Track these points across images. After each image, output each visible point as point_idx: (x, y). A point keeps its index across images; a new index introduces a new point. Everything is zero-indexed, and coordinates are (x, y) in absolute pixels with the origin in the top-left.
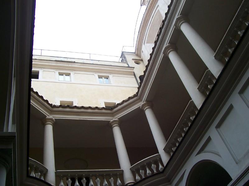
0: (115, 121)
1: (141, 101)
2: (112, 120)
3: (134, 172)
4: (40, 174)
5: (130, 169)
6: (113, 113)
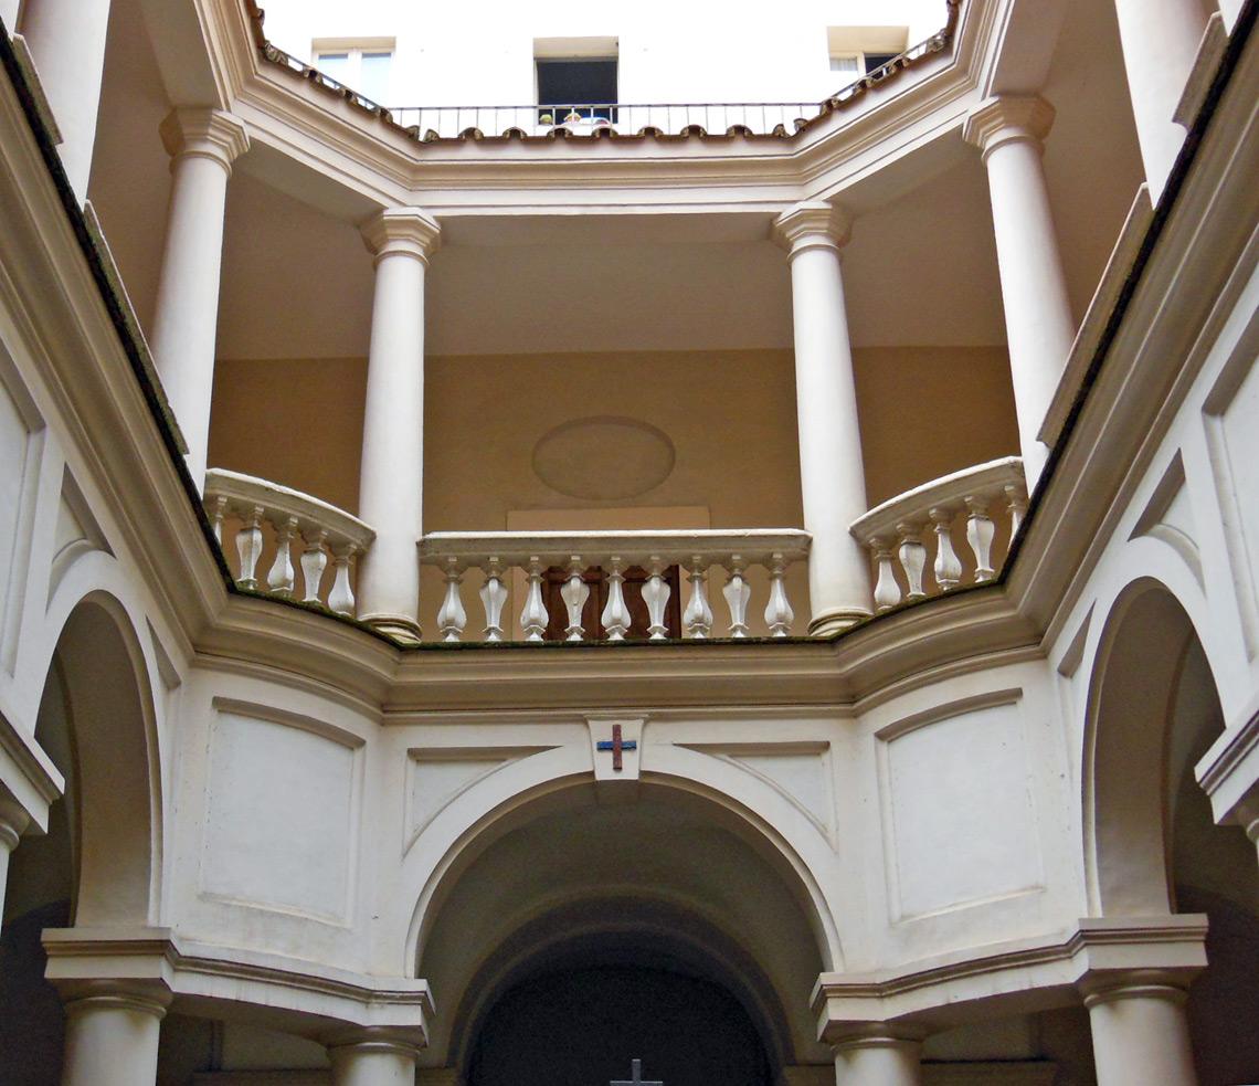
0: (803, 217)
1: (973, 85)
2: (788, 212)
3: (873, 547)
4: (323, 559)
5: (853, 532)
6: (798, 163)
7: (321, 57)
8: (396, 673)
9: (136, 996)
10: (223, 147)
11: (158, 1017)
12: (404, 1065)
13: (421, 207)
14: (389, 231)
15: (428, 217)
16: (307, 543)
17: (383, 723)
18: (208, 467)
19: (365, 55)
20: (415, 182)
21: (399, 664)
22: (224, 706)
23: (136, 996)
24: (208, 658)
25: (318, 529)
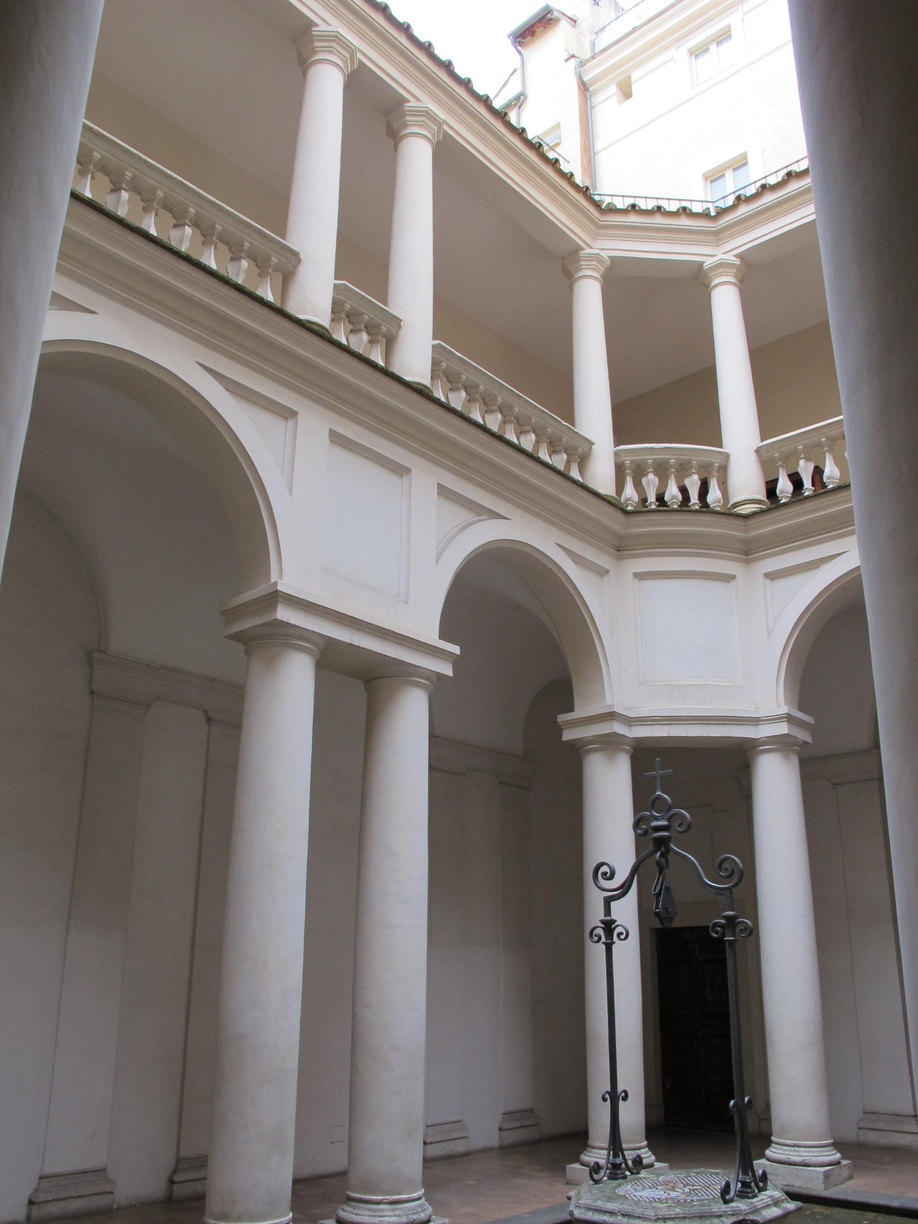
7: (712, 182)
8: (746, 532)
9: (610, 743)
10: (593, 269)
11: (625, 751)
12: (786, 757)
13: (724, 253)
14: (710, 275)
15: (731, 258)
16: (687, 470)
17: (748, 562)
18: (615, 447)
19: (734, 170)
20: (719, 240)
21: (746, 526)
22: (639, 576)
23: (610, 743)
24: (625, 553)
25: (690, 462)
